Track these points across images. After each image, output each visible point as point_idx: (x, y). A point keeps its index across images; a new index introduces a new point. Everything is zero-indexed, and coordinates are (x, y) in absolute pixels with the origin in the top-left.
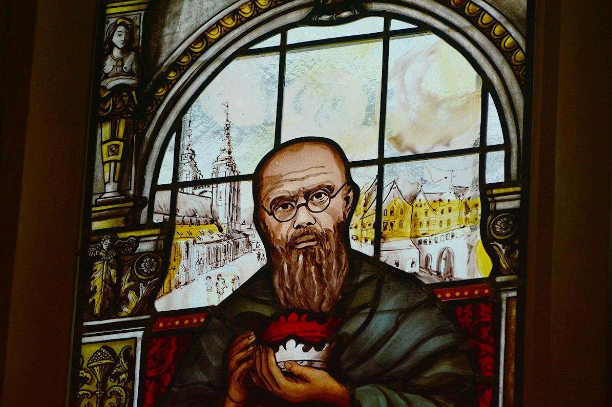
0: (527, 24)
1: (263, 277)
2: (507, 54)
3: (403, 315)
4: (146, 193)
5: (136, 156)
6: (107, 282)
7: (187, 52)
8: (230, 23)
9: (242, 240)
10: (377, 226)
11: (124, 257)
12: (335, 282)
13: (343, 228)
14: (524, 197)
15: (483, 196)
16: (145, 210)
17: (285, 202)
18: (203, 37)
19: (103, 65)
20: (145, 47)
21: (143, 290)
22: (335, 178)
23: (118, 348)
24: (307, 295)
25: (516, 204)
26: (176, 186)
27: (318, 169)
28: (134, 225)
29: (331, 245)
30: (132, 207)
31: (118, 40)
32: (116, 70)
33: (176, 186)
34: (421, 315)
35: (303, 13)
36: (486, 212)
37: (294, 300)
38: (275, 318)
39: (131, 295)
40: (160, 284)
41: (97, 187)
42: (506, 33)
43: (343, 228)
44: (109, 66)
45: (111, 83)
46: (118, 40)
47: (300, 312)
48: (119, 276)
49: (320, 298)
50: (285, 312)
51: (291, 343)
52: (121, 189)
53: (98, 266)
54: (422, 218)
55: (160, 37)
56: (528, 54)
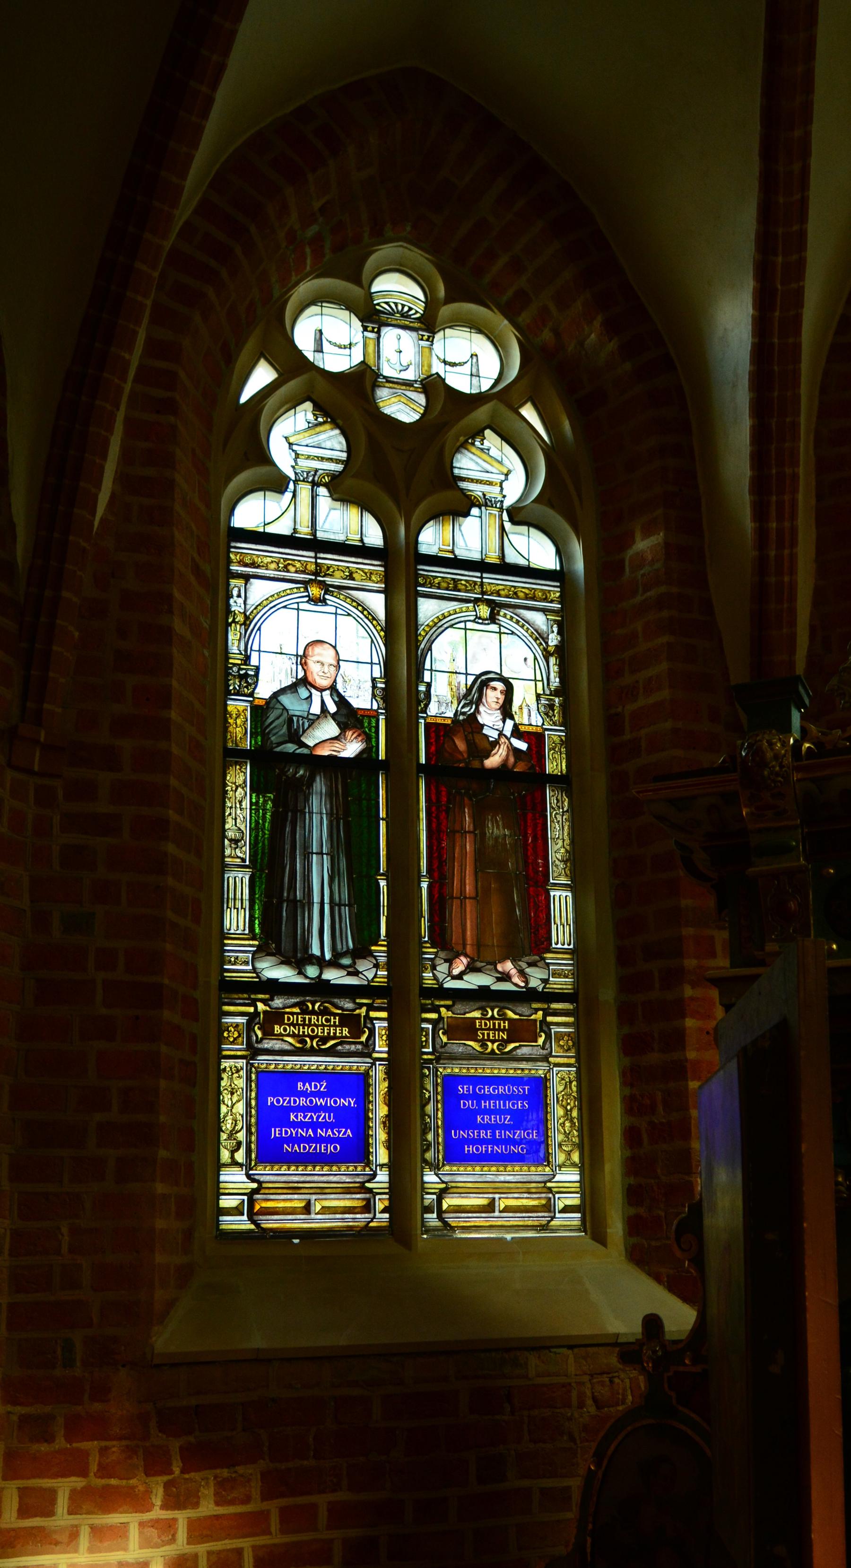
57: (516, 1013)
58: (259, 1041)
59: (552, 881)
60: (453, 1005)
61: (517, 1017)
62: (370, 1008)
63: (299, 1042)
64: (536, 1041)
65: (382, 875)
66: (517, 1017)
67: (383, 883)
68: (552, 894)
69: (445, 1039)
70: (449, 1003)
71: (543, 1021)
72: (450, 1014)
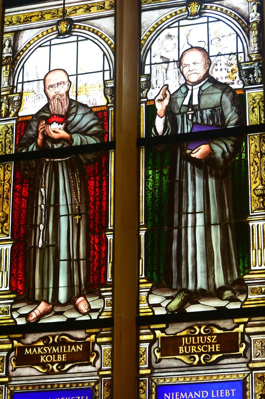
0: (115, 38)
1: (47, 105)
2: (109, 45)
3: (84, 115)
4: (15, 85)
5: (12, 74)
6: (6, 108)
7: (25, 47)
8: (36, 39)
9: (41, 96)
10: (76, 92)
11: (10, 102)
12: (66, 107)
13: (67, 93)
14: (115, 83)
15: (104, 83)
16: (15, 89)
17: (51, 86)
18: (29, 43)
19: (2, 51)
20: (14, 46)
21: (15, 110)
22: (66, 80)
23: (9, 126)
24: (58, 111)
25: (113, 85)
26: (23, 83)
27: (60, 77)
28: (12, 93)
29: (65, 97)
30: (12, 88)
31: (7, 44)
32: (7, 52)
33: (23, 83)
34: (88, 115)
35: (56, 36)
36: (105, 87)
37: (56, 112)
38: (50, 117)
39: (12, 112)
40: (19, 109)
41: (2, 83)
42: (109, 40)
43: (67, 93)
44: (5, 51)
45: (5, 56)
46: (7, 44)
47: (57, 115)
48: (9, 107)
49: (62, 111)
50: (52, 115)
51: (55, 123)
52: (8, 84)
53: (3, 104)
54: (88, 89)
55: (17, 44)
56: (115, 45)
57: (220, 328)
58: (14, 370)
59: (251, 214)
60: (167, 327)
61: (222, 332)
62: (98, 335)
63: (44, 368)
64: (239, 352)
65: (110, 230)
66: (222, 332)
67: (110, 237)
68: (251, 224)
69: (158, 355)
70: (164, 326)
71: (244, 333)
72: (164, 335)
